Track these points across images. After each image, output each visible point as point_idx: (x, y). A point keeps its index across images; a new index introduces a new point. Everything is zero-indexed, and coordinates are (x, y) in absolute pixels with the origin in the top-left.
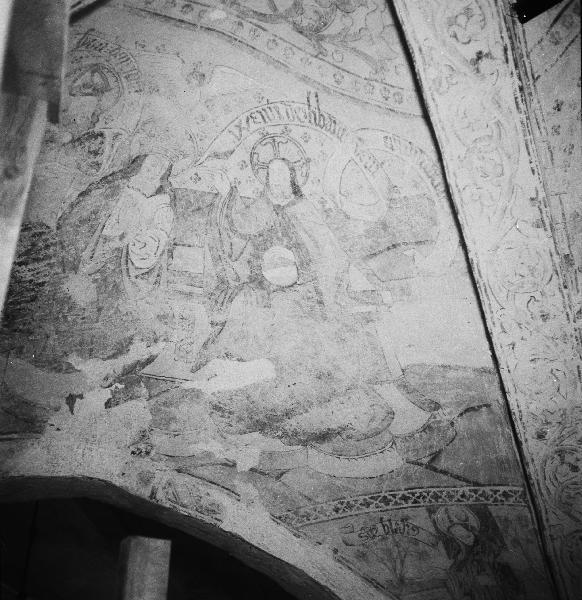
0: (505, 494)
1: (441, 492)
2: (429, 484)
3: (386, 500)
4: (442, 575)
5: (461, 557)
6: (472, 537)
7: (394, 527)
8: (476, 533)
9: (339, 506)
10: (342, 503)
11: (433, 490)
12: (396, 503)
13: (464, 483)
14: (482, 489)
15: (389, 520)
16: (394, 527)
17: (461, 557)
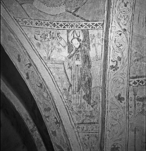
0: (96, 25)
1: (74, 24)
2: (71, 21)
3: (54, 25)
4: (64, 59)
5: (72, 53)
6: (79, 44)
7: (54, 36)
8: (81, 42)
9: (38, 22)
10: (39, 22)
11: (71, 23)
12: (58, 27)
13: (83, 21)
14: (89, 23)
15: (53, 33)
16: (54, 36)
17: (72, 53)
